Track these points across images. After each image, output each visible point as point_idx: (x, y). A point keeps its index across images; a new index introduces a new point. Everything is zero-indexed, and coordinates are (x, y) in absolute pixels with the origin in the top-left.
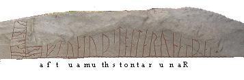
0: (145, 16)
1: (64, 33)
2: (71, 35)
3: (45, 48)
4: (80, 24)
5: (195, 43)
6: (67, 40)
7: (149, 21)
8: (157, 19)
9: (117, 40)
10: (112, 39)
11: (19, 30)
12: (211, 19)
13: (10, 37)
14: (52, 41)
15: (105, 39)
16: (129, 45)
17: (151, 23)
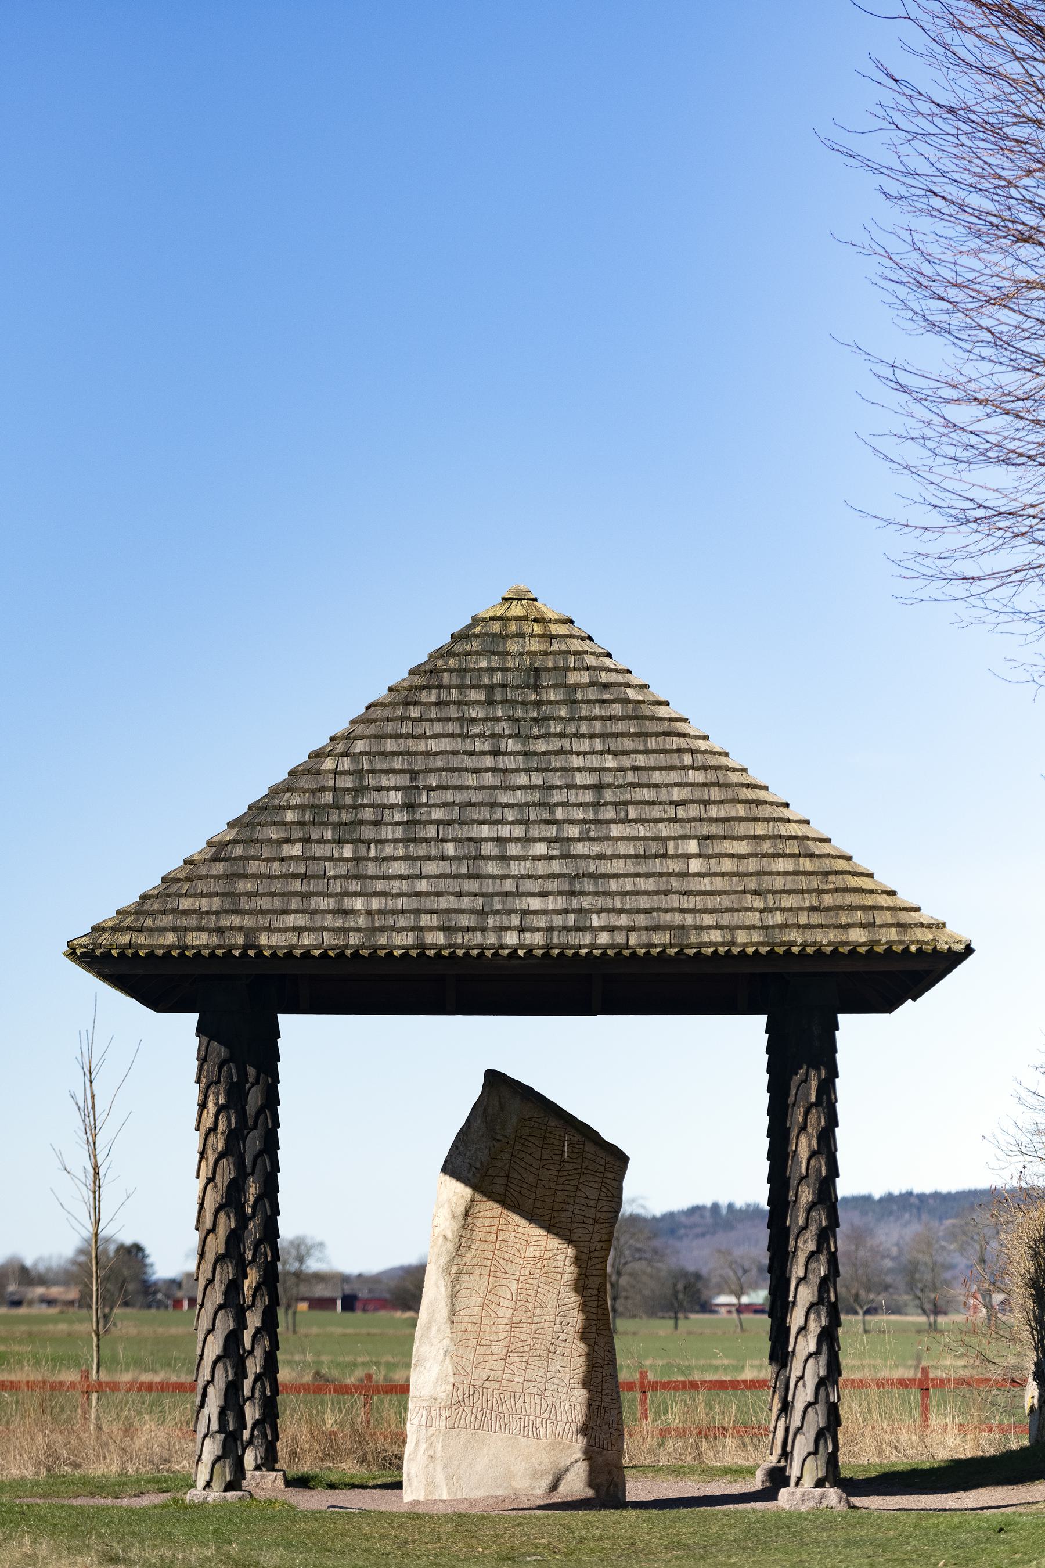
0: (441, 1239)
1: (442, 1352)
2: (446, 1342)
3: (459, 1379)
4: (434, 1330)
5: (489, 1172)
6: (453, 1348)
7: (449, 1235)
8: (448, 1223)
9: (466, 1277)
10: (464, 1285)
11: (424, 1418)
12: (461, 1149)
13: (431, 1431)
14: (450, 1370)
16: (476, 1261)
17: (452, 1231)
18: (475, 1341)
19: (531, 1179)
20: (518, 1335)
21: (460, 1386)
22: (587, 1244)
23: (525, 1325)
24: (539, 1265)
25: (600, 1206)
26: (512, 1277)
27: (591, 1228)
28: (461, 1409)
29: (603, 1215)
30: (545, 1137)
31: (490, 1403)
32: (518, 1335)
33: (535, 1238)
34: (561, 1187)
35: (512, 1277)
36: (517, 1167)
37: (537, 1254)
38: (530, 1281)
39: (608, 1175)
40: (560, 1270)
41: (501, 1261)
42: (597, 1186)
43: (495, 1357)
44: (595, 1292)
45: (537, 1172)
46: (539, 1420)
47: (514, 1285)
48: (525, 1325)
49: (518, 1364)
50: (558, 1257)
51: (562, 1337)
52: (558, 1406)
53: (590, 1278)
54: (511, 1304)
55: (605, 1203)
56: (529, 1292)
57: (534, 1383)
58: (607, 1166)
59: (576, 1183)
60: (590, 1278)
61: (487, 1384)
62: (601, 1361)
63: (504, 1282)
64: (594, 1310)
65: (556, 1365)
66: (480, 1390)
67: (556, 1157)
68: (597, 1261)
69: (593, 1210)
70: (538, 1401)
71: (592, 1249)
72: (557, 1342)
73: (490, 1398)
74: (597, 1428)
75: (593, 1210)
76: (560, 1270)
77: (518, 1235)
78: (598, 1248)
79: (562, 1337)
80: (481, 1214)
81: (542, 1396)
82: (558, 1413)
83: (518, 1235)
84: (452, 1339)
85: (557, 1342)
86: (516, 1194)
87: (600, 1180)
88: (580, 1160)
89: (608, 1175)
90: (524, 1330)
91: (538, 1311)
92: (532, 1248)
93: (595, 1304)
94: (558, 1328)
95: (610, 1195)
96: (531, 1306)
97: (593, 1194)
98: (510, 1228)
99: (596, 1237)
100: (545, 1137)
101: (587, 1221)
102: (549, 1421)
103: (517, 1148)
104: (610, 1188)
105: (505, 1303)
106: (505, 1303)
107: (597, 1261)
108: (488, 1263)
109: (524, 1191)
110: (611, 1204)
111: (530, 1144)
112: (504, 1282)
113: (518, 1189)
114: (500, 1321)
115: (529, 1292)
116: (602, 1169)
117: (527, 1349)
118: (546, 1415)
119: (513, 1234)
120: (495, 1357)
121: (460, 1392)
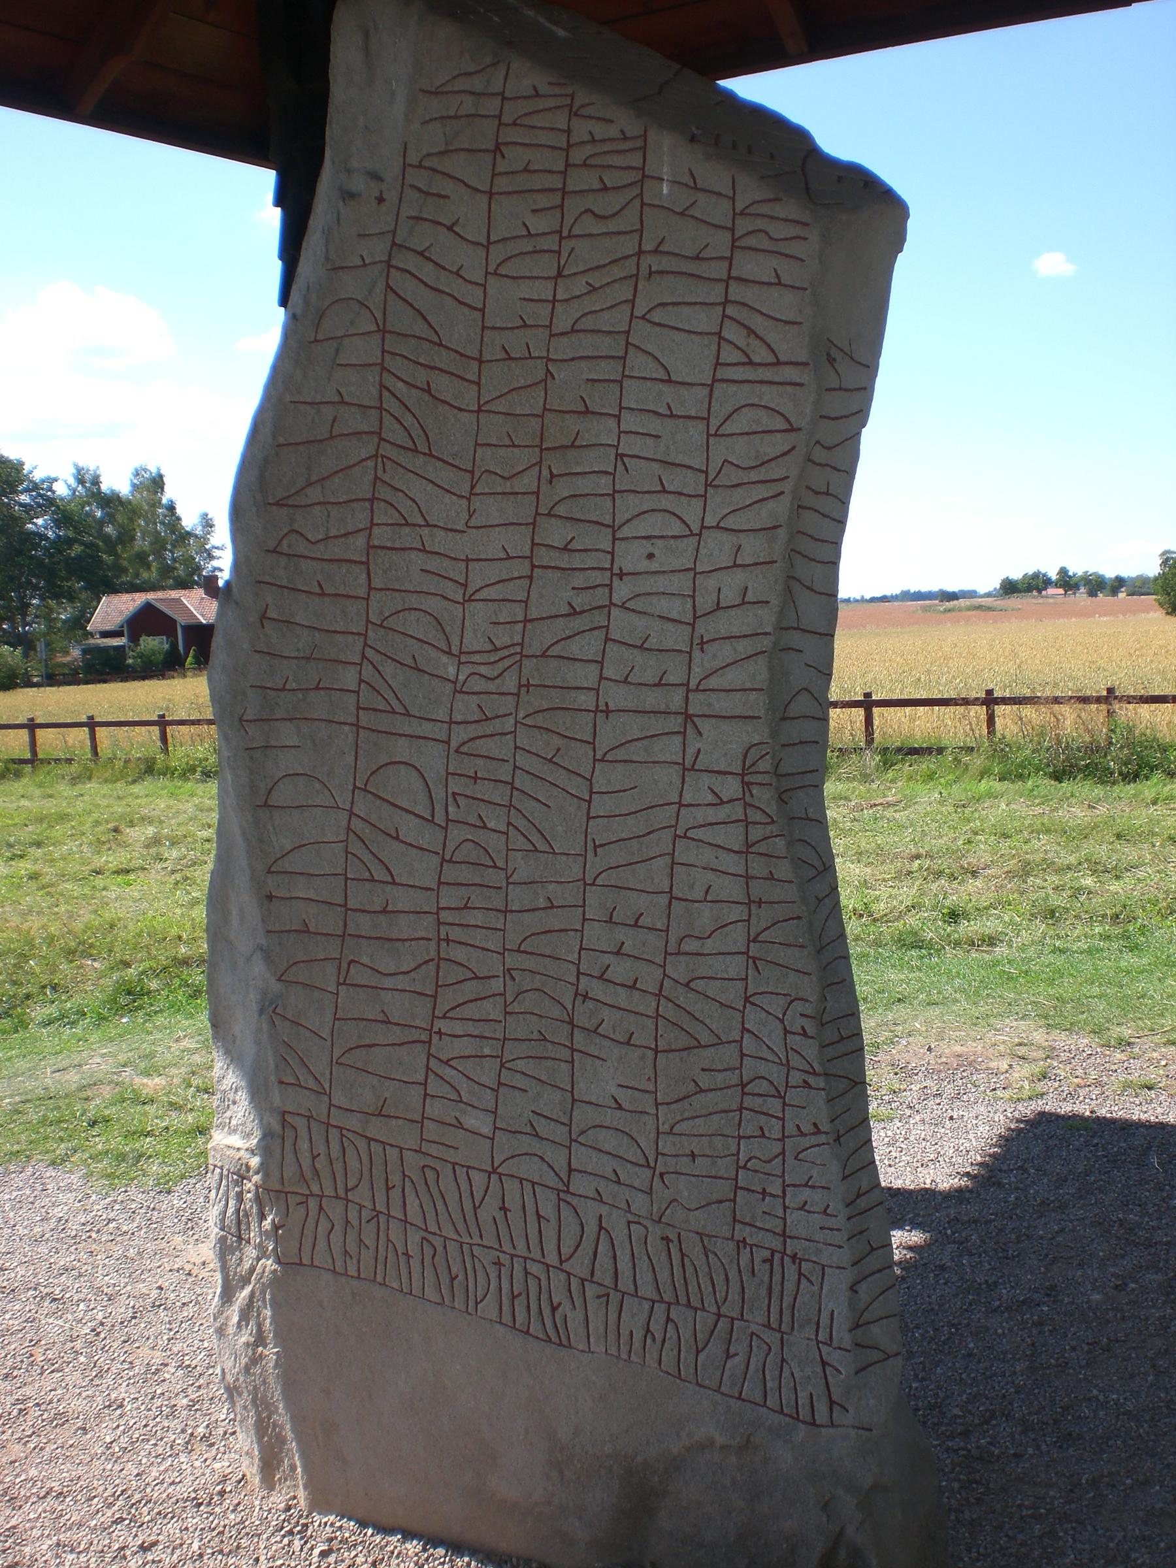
2: (258, 967)
9: (287, 734)
15: (284, 795)
18: (331, 968)
19: (460, 331)
20: (459, 953)
21: (301, 1123)
22: (681, 583)
23: (477, 918)
24: (510, 682)
25: (720, 411)
26: (426, 729)
27: (692, 512)
28: (313, 1204)
29: (740, 452)
30: (498, 149)
31: (396, 1194)
32: (459, 953)
33: (493, 572)
34: (563, 348)
35: (426, 729)
36: (408, 287)
37: (503, 638)
38: (483, 746)
39: (747, 266)
40: (586, 700)
41: (388, 669)
42: (705, 320)
43: (397, 1035)
44: (731, 788)
45: (474, 296)
46: (557, 1279)
47: (433, 760)
48: (477, 918)
49: (468, 1066)
50: (574, 648)
51: (620, 970)
52: (620, 1234)
53: (705, 725)
54: (429, 837)
55: (743, 394)
56: (483, 790)
57: (527, 1143)
58: (743, 226)
59: (618, 319)
60: (705, 725)
61: (376, 1128)
62: (774, 1073)
63: (402, 750)
64: (733, 864)
65: (603, 1080)
66: (362, 1144)
67: (539, 224)
68: (726, 652)
69: (696, 432)
70: (547, 1210)
71: (705, 603)
72: (597, 989)
73: (395, 1179)
74: (772, 1338)
75: (696, 432)
76: (586, 700)
77: (434, 564)
78: (730, 596)
79: (620, 970)
80: (315, 494)
81: (563, 1192)
82: (624, 1265)
83: (434, 564)
84: (268, 957)
85: (597, 989)
86: (412, 397)
87: (716, 293)
88: (629, 220)
89: (747, 266)
90: (478, 938)
91: (523, 867)
92: (479, 613)
93: (733, 837)
94: (596, 935)
95: (761, 354)
96: (495, 843)
97: (691, 360)
98: (408, 537)
99: (717, 548)
100: (498, 149)
101: (674, 480)
102: (591, 1291)
103: (407, 211)
104: (757, 323)
105: (409, 828)
106: (409, 828)
107: (726, 652)
108: (349, 678)
109: (444, 386)
110: (769, 396)
111: (448, 187)
112: (402, 750)
113: (421, 377)
114: (402, 899)
115: (483, 790)
116: (720, 243)
117: (492, 1009)
118: (578, 1266)
119: (418, 560)
120: (397, 1035)
121: (304, 1145)
